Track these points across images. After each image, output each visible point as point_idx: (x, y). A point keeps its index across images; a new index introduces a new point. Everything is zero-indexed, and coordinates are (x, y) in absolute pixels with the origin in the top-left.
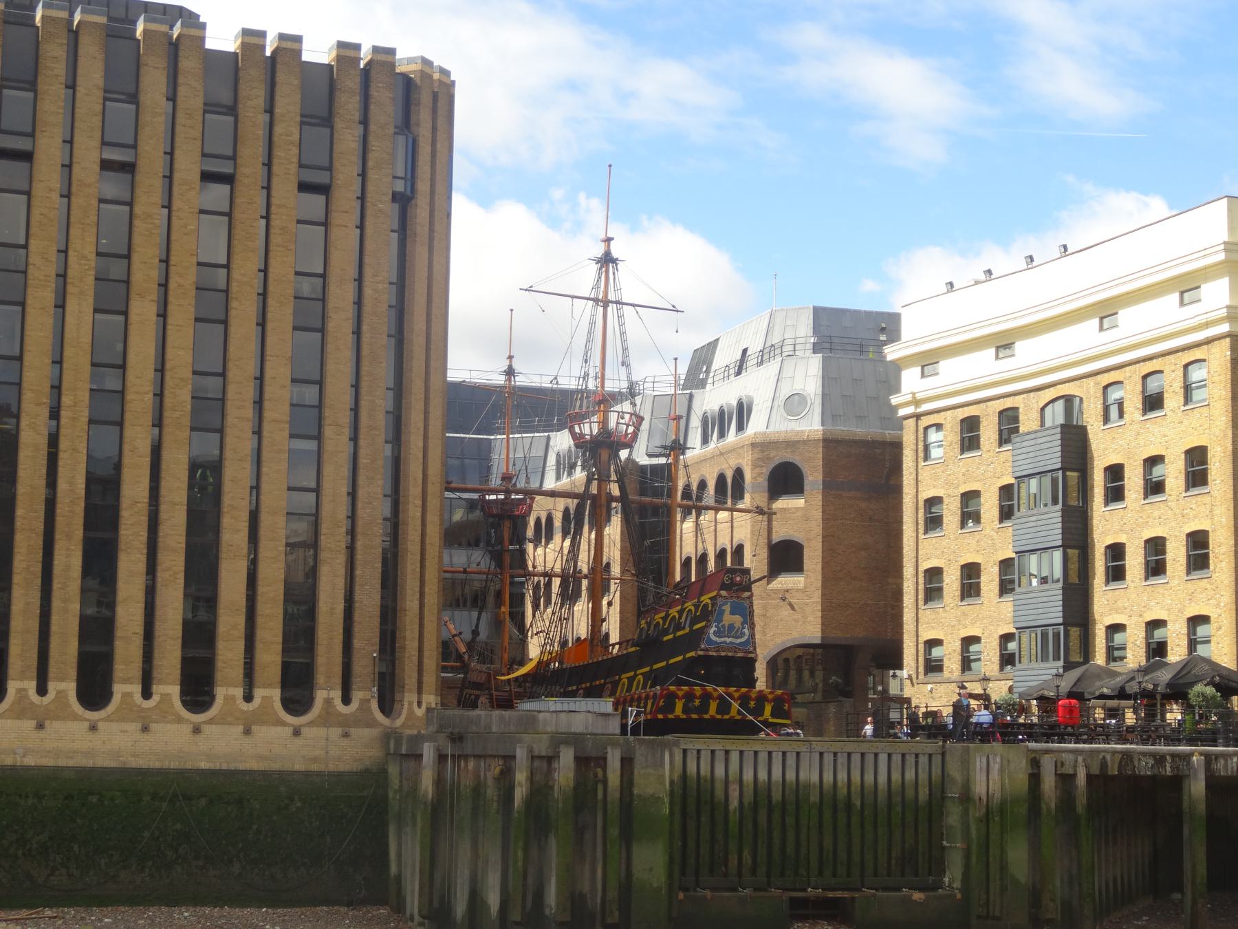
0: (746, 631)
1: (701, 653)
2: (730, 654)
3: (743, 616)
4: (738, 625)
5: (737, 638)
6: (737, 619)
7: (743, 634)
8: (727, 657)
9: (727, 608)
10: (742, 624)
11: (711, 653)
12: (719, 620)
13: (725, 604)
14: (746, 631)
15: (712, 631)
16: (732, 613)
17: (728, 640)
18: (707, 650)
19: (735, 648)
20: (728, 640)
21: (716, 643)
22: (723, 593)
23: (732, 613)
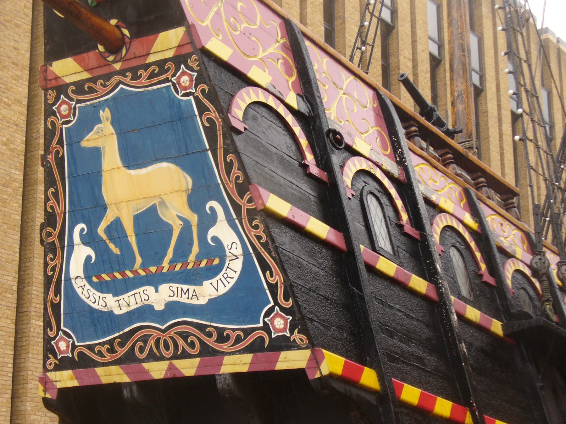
0: (222, 231)
1: (66, 379)
2: (188, 368)
3: (186, 157)
4: (176, 211)
5: (193, 277)
6: (164, 185)
7: (218, 250)
8: (175, 384)
9: (104, 137)
10: (196, 201)
11: (112, 375)
12: (91, 205)
13: (89, 121)
14: (222, 231)
15: (76, 268)
16: (132, 158)
17: (160, 296)
18: (80, 362)
19: (199, 332)
20: (160, 296)
21: (107, 320)
22: (67, 69)
23: (132, 158)
